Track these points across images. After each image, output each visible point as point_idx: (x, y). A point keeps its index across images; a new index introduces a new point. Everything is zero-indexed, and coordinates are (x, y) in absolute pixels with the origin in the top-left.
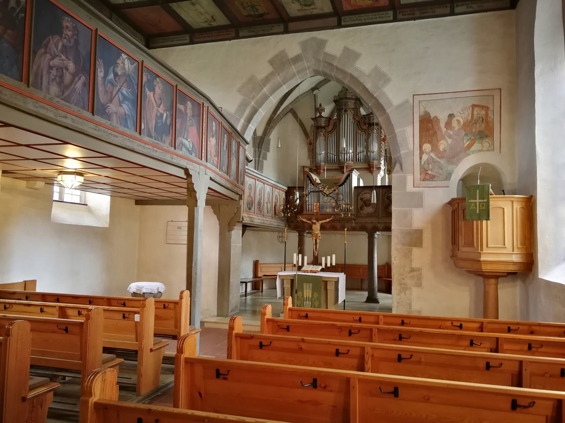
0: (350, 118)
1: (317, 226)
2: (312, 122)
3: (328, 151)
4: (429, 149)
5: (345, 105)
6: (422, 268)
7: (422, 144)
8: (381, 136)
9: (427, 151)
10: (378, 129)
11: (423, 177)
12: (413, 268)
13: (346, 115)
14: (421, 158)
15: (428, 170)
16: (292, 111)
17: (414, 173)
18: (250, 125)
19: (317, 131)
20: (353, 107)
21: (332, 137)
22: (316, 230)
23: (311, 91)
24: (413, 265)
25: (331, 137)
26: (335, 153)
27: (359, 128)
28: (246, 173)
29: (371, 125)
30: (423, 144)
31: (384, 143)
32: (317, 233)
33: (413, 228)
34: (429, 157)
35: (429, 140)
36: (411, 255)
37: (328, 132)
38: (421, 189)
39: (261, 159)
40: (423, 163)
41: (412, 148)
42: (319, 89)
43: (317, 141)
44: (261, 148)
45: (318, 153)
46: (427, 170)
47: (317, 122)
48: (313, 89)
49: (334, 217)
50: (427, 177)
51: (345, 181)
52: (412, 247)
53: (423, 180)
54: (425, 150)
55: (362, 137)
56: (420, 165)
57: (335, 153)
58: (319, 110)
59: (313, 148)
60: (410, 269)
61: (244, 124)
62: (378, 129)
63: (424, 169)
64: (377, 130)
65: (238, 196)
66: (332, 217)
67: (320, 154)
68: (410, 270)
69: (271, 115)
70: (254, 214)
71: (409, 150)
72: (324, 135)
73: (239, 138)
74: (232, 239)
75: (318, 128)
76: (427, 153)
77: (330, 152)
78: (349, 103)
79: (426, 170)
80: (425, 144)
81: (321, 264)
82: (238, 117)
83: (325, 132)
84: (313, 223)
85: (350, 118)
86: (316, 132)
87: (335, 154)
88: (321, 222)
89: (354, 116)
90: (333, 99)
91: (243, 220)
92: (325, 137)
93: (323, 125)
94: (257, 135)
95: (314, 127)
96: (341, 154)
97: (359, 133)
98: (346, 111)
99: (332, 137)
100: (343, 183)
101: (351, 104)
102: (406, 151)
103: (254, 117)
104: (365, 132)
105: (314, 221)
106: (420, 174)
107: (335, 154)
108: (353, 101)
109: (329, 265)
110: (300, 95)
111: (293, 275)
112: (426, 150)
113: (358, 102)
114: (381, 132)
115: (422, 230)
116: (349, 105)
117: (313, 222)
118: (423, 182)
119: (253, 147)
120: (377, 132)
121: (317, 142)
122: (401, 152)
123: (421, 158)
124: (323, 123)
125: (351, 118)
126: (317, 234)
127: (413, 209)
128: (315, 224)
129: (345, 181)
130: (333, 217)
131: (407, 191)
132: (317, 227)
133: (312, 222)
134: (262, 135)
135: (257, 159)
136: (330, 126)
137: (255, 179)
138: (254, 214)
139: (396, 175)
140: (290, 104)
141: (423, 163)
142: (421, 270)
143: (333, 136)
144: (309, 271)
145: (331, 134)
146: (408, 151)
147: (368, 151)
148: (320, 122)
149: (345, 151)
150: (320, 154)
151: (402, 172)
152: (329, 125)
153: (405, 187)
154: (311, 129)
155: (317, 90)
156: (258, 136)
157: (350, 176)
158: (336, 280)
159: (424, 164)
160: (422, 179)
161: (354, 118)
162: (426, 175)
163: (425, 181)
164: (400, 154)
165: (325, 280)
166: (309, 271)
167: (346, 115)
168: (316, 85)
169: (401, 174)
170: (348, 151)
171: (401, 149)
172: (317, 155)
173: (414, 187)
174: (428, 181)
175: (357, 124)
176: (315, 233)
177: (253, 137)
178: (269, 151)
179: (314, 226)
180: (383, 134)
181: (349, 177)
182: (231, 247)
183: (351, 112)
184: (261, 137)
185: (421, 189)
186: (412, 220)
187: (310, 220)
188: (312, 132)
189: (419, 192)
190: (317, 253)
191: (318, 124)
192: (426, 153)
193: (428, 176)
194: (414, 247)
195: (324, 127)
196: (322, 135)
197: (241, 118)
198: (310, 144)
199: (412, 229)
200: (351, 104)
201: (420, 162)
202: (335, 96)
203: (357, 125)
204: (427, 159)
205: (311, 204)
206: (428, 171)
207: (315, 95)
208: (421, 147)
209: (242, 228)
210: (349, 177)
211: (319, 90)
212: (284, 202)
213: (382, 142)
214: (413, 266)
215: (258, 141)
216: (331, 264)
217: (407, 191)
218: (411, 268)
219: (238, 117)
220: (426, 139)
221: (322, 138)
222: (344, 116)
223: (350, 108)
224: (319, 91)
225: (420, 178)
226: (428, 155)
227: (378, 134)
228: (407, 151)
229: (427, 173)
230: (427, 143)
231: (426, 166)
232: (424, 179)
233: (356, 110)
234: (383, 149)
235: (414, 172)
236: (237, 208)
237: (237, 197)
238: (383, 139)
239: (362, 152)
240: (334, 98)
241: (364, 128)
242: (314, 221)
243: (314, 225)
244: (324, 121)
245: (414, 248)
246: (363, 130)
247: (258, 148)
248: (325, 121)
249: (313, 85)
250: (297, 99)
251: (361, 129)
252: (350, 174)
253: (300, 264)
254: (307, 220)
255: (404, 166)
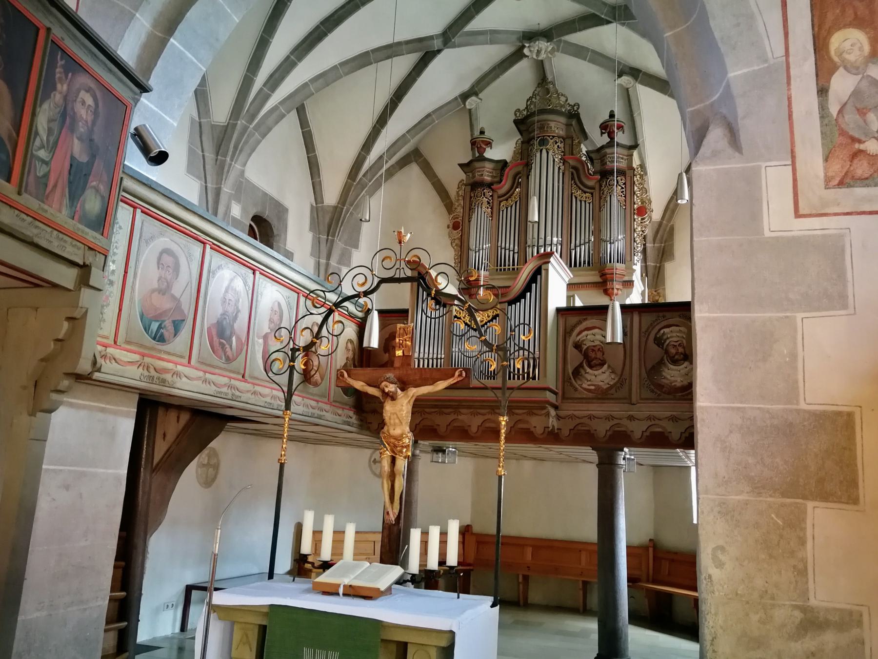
0: (554, 160)
1: (398, 407)
2: (461, 175)
3: (500, 243)
4: (861, 49)
5: (542, 128)
6: (865, 611)
7: (824, 33)
8: (634, 204)
9: (852, 57)
10: (625, 184)
11: (837, 168)
12: (812, 609)
13: (544, 151)
14: (823, 91)
15: (863, 138)
16: (416, 156)
17: (793, 158)
18: (172, 40)
19: (473, 195)
20: (562, 133)
21: (509, 209)
22: (397, 421)
23: (459, 100)
24: (811, 595)
25: (507, 208)
26: (516, 247)
27: (576, 184)
28: (124, 191)
29: (605, 174)
30: (830, 33)
31: (640, 219)
32: (397, 432)
33: (803, 406)
34: (865, 84)
35: (856, 14)
36: (802, 542)
37: (499, 197)
38: (831, 225)
39: (333, 262)
40: (834, 110)
41: (780, 51)
42: (480, 95)
43: (473, 219)
44: (333, 236)
45: (474, 247)
46: (856, 135)
47: (473, 174)
48: (465, 96)
49: (464, 374)
50: (861, 168)
51: (528, 288)
52: (805, 498)
53: (841, 184)
54: (840, 55)
55: (584, 208)
56: (822, 117)
57: (516, 247)
58: (479, 144)
59: (461, 236)
60: (798, 615)
61: (151, 36)
62: (625, 184)
63: (843, 133)
64: (622, 188)
65: (73, 272)
66: (457, 373)
67: (477, 250)
68: (797, 621)
69: (360, 154)
70: (189, 362)
71: (766, 61)
72: (489, 203)
73: (51, 13)
74: (48, 443)
75: (475, 186)
76: (851, 69)
77: (503, 246)
78: (552, 124)
79: (854, 140)
80: (840, 29)
81: (404, 564)
82: (128, 8)
83: (491, 196)
84: (386, 395)
85: (554, 160)
86: (471, 197)
87: (516, 251)
88: (415, 392)
89: (564, 155)
90: (514, 117)
91: (99, 370)
92: (491, 208)
93: (487, 178)
94: (325, 204)
95: (465, 185)
96: (531, 249)
97: (576, 198)
98: (543, 142)
99: (509, 209)
100: (522, 296)
101: (557, 126)
102: (752, 68)
103: (188, 14)
104: (592, 194)
105: (391, 388)
106: (826, 159)
107: (516, 251)
108: (563, 120)
109: (433, 564)
110: (434, 111)
111: (266, 610)
112: (847, 56)
113: (574, 122)
114: (634, 193)
115: (850, 415)
116: (551, 127)
117: (387, 390)
118: (844, 191)
119: (312, 228)
120: (622, 192)
121: (472, 223)
122: (731, 75)
123: (823, 91)
124: (488, 176)
125: (556, 160)
126: (399, 438)
127: (799, 316)
128: (393, 397)
129: (528, 288)
130: (460, 375)
131: (767, 234)
132: (401, 410)
133: (383, 391)
134: (338, 203)
135: (323, 261)
136: (503, 181)
137: (204, 243)
138: (189, 362)
139: (712, 168)
140: (408, 132)
141: (834, 110)
142: (860, 624)
143: (511, 207)
144: (341, 591)
145: (507, 200)
146: (766, 65)
147: (599, 241)
148: (479, 171)
149: (540, 240)
150: (477, 250)
151: (737, 154)
152: (501, 181)
153: (755, 217)
154: (458, 192)
155: (474, 98)
156: (328, 206)
157: (543, 272)
158: (444, 643)
159: (840, 112)
160: (836, 182)
161: (564, 161)
162: (855, 161)
163: (850, 186)
164: (728, 81)
165: (396, 639)
166: (341, 591)
167: (544, 151)
168: (473, 87)
169: (735, 164)
170: (549, 238)
171: (729, 61)
172: (470, 251)
173: (798, 215)
174: (868, 186)
175: (572, 174)
176: (392, 432)
177: (312, 206)
178: (356, 246)
179: (389, 408)
180: (638, 197)
181: (538, 275)
182: (44, 479)
183: (556, 146)
184: (335, 208)
185: (831, 225)
186: (795, 369)
187: (377, 386)
188: (460, 198)
189: (824, 236)
190: (397, 511)
191: (475, 177)
192: (846, 68)
193: (865, 163)
194: (814, 499)
195: (490, 185)
196: (485, 205)
197: (137, 10)
198: (456, 226)
199: (798, 411)
200: (557, 126)
201: (823, 108)
202: (518, 110)
203: (573, 179)
204: (856, 94)
205: (426, 356)
206: (860, 142)
207: (470, 110)
208: (820, 45)
209: (136, 410)
210: (539, 277)
211: (478, 98)
212: (351, 353)
213: (635, 217)
214: (813, 602)
215: (327, 220)
216: (442, 563)
217: (767, 234)
218: (804, 609)
219: (128, 8)
220: (843, 11)
221: (484, 210)
222: (538, 155)
223: (554, 137)
224: (480, 101)
225: (826, 176)
226: (860, 76)
227: (625, 197)
228: (756, 68)
229: (856, 154)
230: (850, 25)
231: (851, 120)
232: (848, 180)
233: (569, 141)
234: (638, 235)
235: (793, 152)
236: (70, 319)
237: (66, 276)
238: (638, 209)
239: (584, 244)
240: (516, 115)
241: (590, 183)
242: (391, 388)
243: (390, 402)
244: (491, 171)
245: (817, 504)
246: (584, 189)
247: (328, 236)
248: (493, 169)
249: (466, 87)
250: (427, 121)
251: (582, 187)
252: (543, 267)
253: (326, 554)
254: (370, 385)
255: (747, 128)
